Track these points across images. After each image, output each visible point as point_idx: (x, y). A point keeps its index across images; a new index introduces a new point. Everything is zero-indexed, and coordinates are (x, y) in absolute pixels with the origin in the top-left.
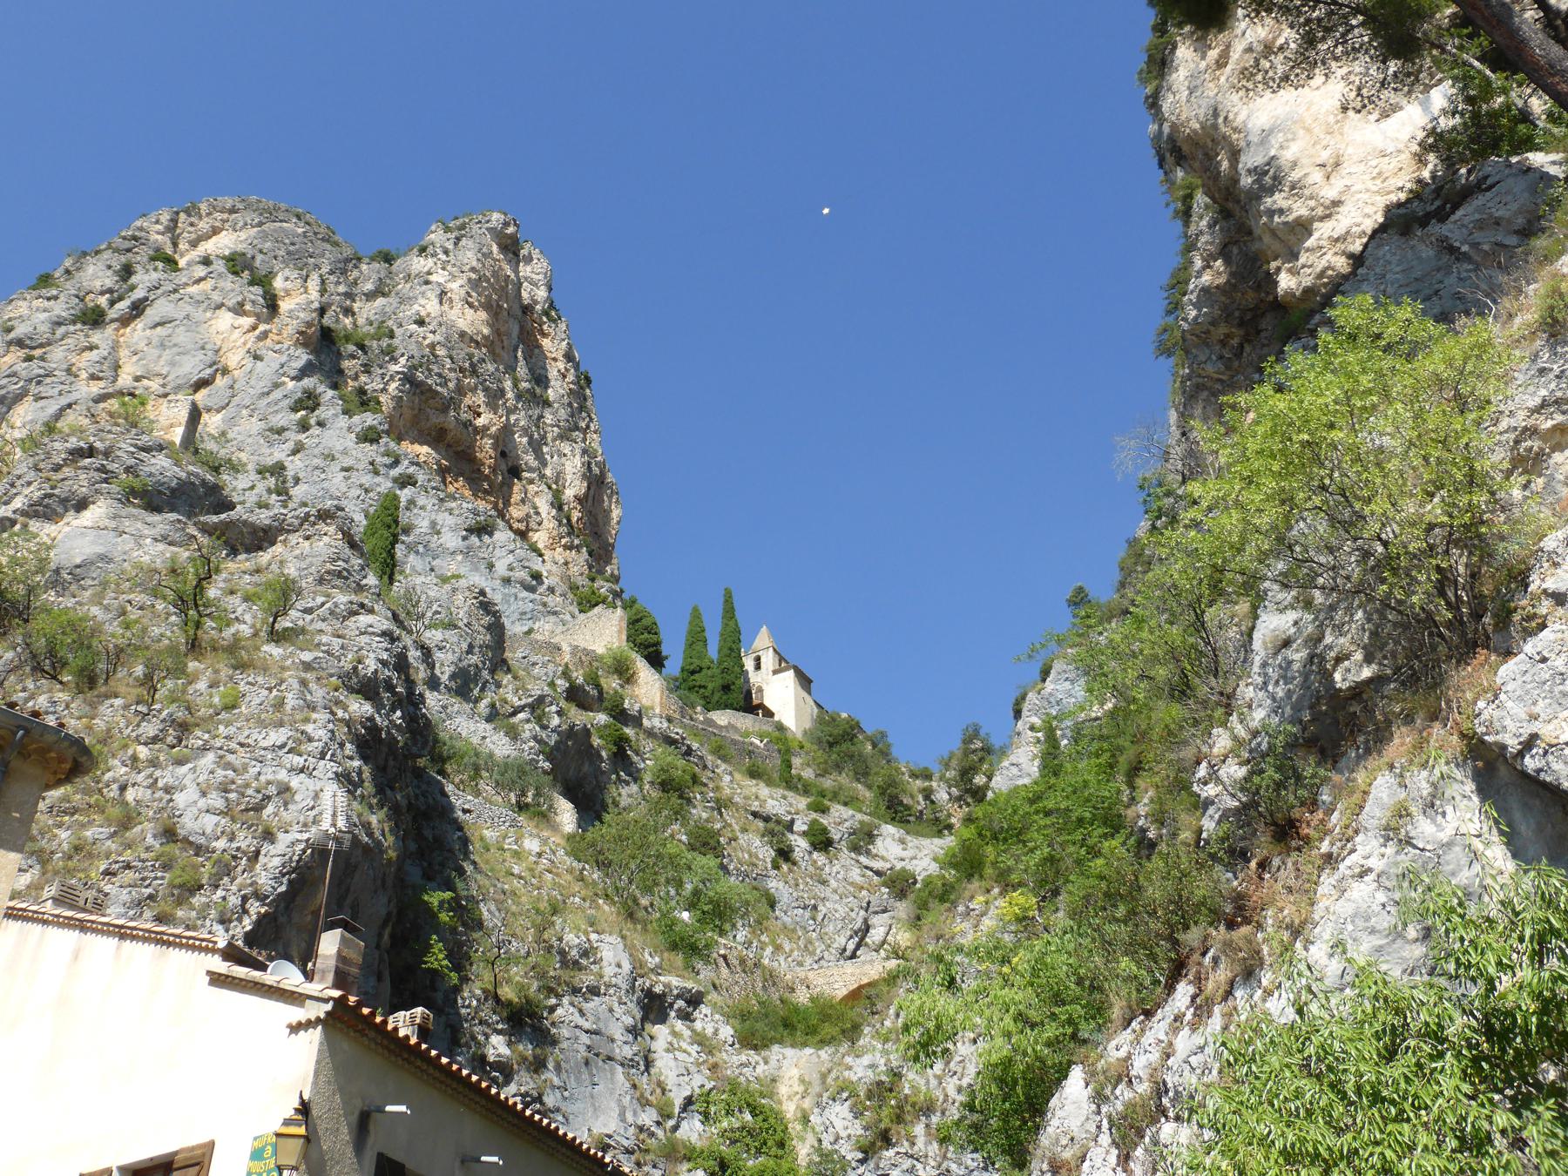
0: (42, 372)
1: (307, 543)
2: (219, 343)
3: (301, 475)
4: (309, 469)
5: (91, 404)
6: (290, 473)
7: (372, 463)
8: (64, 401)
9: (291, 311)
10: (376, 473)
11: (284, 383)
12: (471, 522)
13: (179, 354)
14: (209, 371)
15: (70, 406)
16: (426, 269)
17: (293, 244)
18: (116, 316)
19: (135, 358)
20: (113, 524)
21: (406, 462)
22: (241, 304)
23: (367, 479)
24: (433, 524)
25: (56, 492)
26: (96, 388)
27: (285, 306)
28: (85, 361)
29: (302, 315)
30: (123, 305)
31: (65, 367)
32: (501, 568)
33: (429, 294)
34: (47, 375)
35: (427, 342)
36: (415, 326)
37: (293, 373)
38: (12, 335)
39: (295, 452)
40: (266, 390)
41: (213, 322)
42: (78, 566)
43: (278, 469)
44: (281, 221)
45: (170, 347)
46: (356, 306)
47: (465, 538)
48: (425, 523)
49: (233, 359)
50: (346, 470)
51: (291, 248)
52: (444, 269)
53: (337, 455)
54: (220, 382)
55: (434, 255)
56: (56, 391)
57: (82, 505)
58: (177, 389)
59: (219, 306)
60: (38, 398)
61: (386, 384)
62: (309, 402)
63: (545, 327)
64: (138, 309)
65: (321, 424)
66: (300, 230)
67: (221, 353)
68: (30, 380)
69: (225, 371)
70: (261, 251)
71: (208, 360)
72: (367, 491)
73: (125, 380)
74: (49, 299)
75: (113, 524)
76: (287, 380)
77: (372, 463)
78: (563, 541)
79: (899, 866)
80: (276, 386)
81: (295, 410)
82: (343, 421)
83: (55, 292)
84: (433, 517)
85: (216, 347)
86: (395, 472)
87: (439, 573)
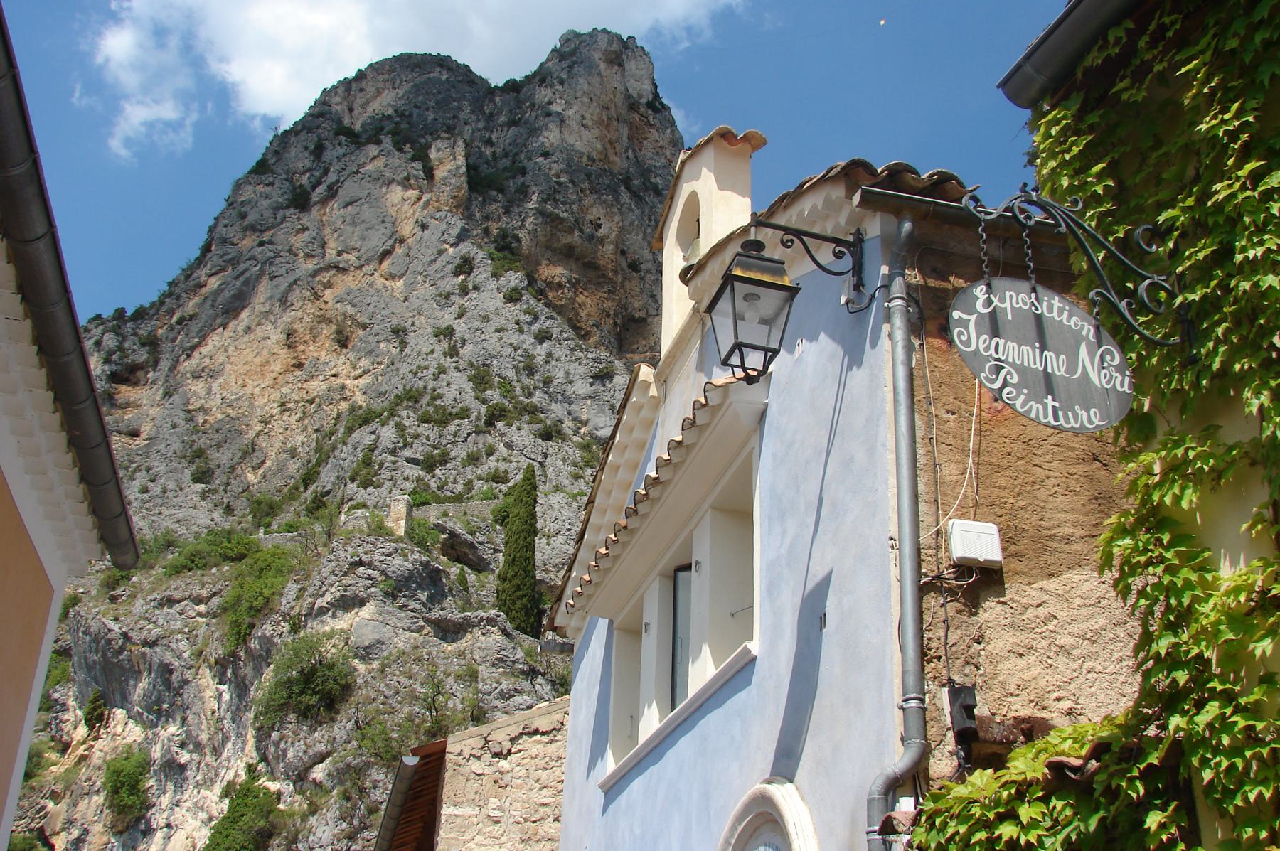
0: (271, 254)
1: (483, 638)
2: (394, 214)
3: (466, 338)
4: (472, 331)
5: (310, 279)
6: (458, 336)
7: (517, 323)
8: (291, 278)
9: (444, 179)
10: (521, 331)
11: (446, 250)
12: (596, 370)
13: (367, 229)
14: (390, 242)
15: (295, 282)
16: (547, 100)
17: (439, 92)
18: (317, 199)
19: (335, 235)
20: (380, 618)
21: (543, 318)
22: (407, 178)
23: (515, 338)
24: (567, 373)
25: (348, 593)
26: (311, 265)
27: (440, 173)
28: (299, 241)
29: (453, 181)
30: (321, 189)
31: (287, 248)
33: (550, 125)
34: (276, 257)
35: (553, 172)
36: (541, 159)
37: (452, 240)
38: (246, 222)
39: (460, 316)
40: (433, 258)
41: (388, 196)
42: (367, 647)
43: (449, 332)
44: (429, 73)
45: (360, 223)
46: (494, 137)
47: (592, 385)
48: (561, 374)
49: (407, 228)
50: (498, 331)
51: (440, 97)
52: (561, 98)
53: (491, 316)
54: (399, 251)
55: (552, 86)
56: (284, 270)
57: (362, 603)
58: (369, 261)
59: (391, 182)
60: (272, 278)
61: (523, 220)
63: (651, 119)
64: (332, 193)
65: (476, 288)
66: (444, 77)
67: (397, 223)
68: (264, 263)
69: (402, 241)
70: (416, 106)
71: (388, 232)
73: (331, 255)
74: (267, 185)
75: (380, 618)
76: (447, 246)
77: (517, 323)
80: (441, 252)
81: (456, 274)
82: (493, 284)
83: (271, 179)
84: (567, 367)
85: (393, 219)
86: (536, 327)
87: (575, 416)
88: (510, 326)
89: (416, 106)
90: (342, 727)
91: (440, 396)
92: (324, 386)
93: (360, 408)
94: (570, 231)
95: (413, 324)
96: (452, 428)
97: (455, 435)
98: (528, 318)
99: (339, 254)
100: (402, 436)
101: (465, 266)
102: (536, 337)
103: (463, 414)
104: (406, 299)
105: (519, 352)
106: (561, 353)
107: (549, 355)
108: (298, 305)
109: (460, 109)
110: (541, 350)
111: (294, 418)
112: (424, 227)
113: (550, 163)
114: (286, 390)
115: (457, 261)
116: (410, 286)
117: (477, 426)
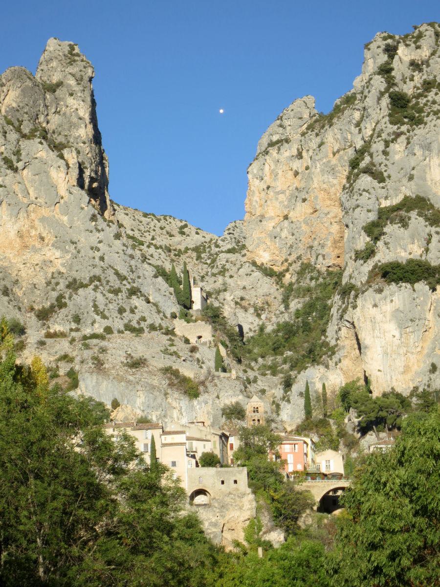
36: (82, 145)
39: (100, 242)
49: (62, 191)
53: (111, 244)
54: (62, 201)
77: (123, 251)
88: (121, 251)
92: (42, 258)
93: (63, 273)
97: (122, 299)
98: (125, 248)
99: (36, 198)
104: (71, 227)
107: (136, 266)
108: (22, 219)
109: (40, 105)
110: (133, 263)
111: (30, 272)
114: (24, 257)
115: (90, 216)
116: (71, 221)
117: (127, 296)
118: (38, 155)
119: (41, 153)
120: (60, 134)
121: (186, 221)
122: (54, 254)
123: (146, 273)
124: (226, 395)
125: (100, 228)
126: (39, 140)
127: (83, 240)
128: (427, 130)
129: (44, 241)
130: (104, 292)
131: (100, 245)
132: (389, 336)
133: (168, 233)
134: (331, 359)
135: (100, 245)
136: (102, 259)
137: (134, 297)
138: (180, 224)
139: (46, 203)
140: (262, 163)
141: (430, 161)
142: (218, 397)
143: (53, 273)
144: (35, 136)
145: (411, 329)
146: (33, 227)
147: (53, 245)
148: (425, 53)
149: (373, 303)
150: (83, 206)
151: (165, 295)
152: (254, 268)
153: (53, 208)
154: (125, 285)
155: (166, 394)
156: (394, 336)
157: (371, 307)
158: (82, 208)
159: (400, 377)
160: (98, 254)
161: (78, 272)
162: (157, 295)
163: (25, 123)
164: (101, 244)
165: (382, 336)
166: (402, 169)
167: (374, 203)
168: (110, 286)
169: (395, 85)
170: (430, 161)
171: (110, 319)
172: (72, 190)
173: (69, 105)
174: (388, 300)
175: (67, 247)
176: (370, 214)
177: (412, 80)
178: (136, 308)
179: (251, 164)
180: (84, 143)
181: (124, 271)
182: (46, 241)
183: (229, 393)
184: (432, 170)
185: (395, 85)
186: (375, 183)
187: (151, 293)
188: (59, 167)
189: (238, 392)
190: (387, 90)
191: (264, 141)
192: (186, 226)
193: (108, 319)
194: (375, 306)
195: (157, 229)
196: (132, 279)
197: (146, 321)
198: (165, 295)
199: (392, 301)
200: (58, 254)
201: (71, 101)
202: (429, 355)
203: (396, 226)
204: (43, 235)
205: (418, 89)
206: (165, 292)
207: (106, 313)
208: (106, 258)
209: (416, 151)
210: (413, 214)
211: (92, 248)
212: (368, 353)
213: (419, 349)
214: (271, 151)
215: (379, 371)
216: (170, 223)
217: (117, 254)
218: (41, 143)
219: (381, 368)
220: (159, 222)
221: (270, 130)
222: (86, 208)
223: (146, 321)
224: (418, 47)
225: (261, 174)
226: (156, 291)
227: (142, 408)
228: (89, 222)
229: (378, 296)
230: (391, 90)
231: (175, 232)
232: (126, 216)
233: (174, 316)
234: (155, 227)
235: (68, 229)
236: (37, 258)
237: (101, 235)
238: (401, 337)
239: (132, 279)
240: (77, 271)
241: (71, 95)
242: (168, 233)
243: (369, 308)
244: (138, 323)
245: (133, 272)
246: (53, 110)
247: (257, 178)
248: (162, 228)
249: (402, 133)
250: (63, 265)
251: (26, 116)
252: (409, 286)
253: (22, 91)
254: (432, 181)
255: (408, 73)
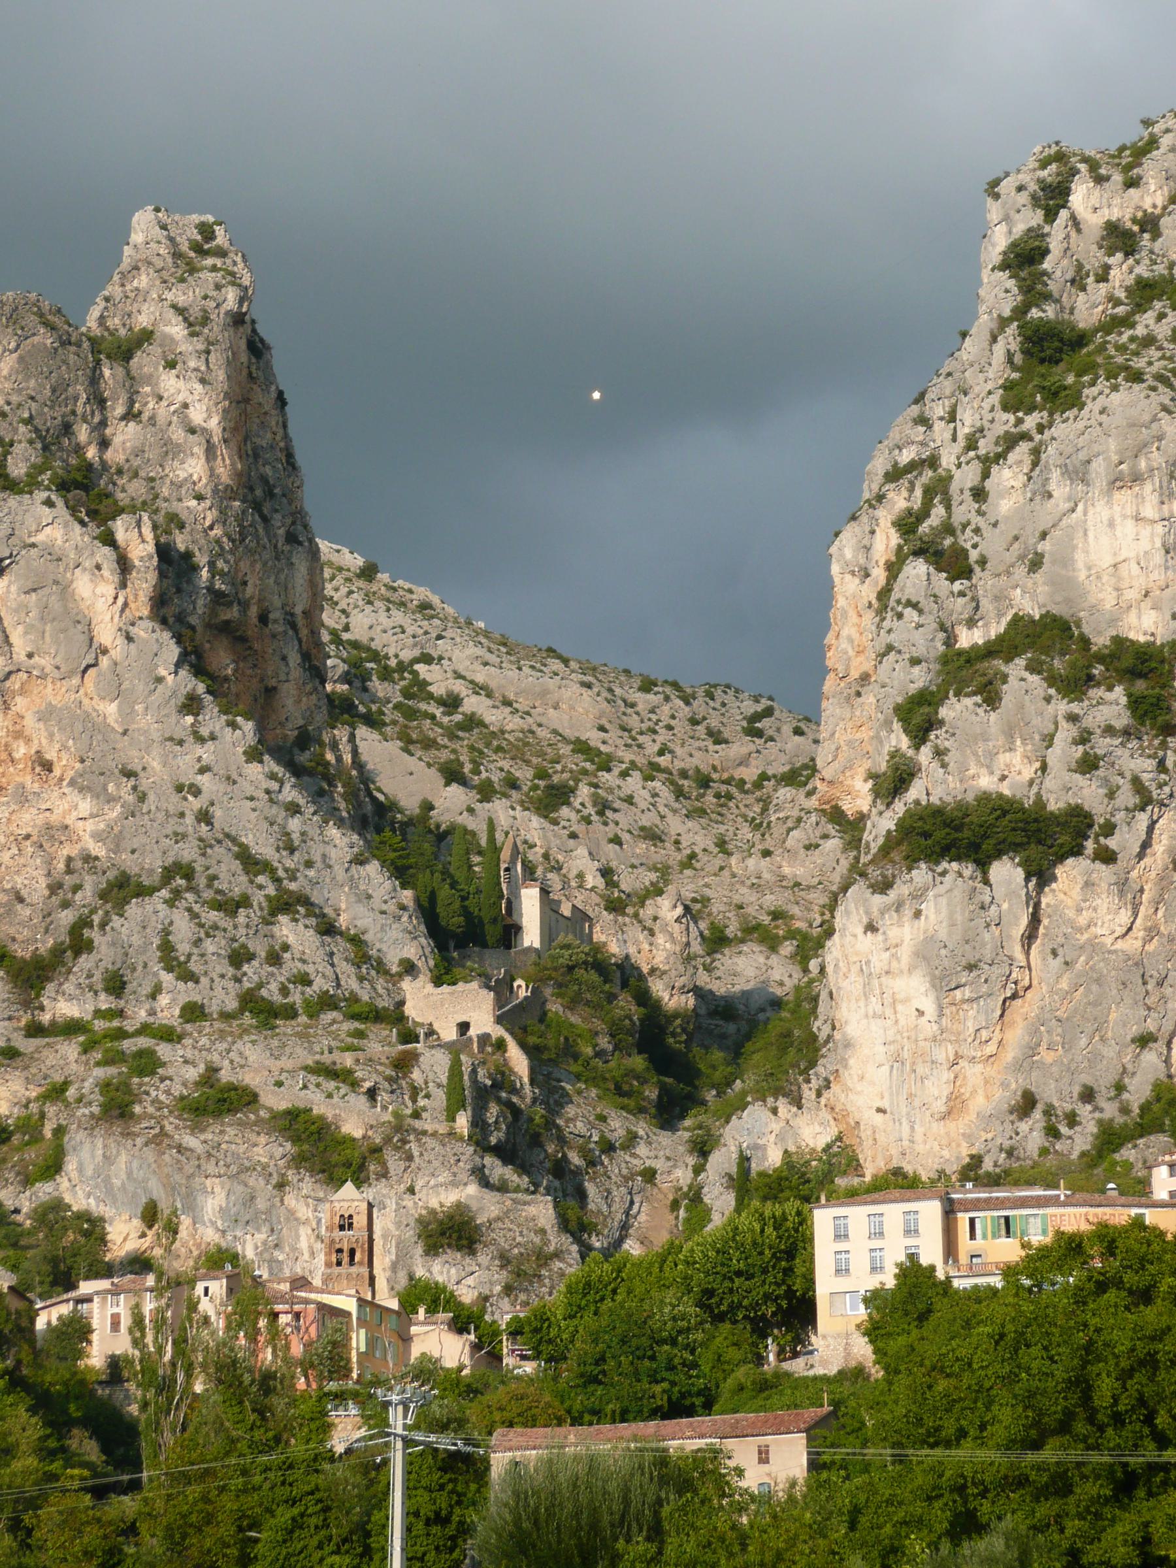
19: (20, 628)
24: (324, 856)
32: (376, 903)
36: (194, 503)
39: (203, 770)
49: (106, 634)
50: (252, 799)
53: (235, 776)
54: (104, 662)
61: (194, 603)
62: (191, 705)
65: (213, 737)
69: (105, 651)
72: (272, 824)
77: (268, 792)
78: (309, 687)
79: (648, 1163)
89: (32, 398)
90: (483, 1258)
91: (214, 878)
92: (40, 820)
93: (97, 858)
94: (229, 605)
95: (144, 769)
96: (242, 916)
97: (247, 926)
98: (274, 786)
99: (30, 656)
100: (202, 926)
101: (191, 705)
102: (287, 810)
103: (244, 902)
104: (125, 733)
105: (276, 828)
106: (313, 832)
107: (303, 834)
109: (76, 399)
110: (294, 824)
112: (129, 639)
113: (204, 510)
115: (181, 699)
116: (127, 714)
117: (263, 918)
118: (40, 538)
119: (48, 530)
120: (136, 475)
121: (771, 699)
122: (76, 807)
123: (333, 854)
124: (432, 1183)
125: (205, 732)
126: (45, 494)
127: (156, 765)
128: (1080, 425)
129: (50, 771)
130: (197, 908)
131: (204, 781)
132: (906, 1013)
133: (710, 733)
134: (808, 1081)
135: (204, 781)
136: (204, 817)
137: (283, 919)
138: (750, 707)
139: (58, 668)
140: (867, 529)
141: (1085, 513)
142: (411, 1190)
143: (69, 859)
144: (39, 485)
145: (967, 992)
146: (18, 735)
147: (72, 783)
148: (1152, 196)
149: (865, 920)
150: (162, 672)
151: (383, 912)
152: (830, 829)
153: (76, 681)
154: (260, 887)
155: (281, 1186)
156: (921, 1013)
157: (860, 930)
158: (160, 680)
159: (938, 1128)
160: (195, 803)
161: (136, 855)
162: (361, 909)
163: (18, 449)
164: (207, 776)
165: (889, 1012)
166: (1016, 538)
167: (932, 640)
168: (218, 892)
169: (1047, 297)
170: (1085, 513)
171: (204, 981)
172: (134, 631)
173: (165, 395)
174: (908, 912)
175: (111, 788)
176: (916, 670)
177: (1103, 278)
178: (286, 947)
179: (837, 535)
180: (200, 498)
181: (263, 847)
182: (57, 772)
183: (441, 1179)
184: (1091, 534)
185: (1047, 297)
186: (941, 581)
187: (343, 906)
188: (98, 567)
189: (464, 1176)
190: (1020, 312)
191: (879, 465)
192: (768, 712)
193: (197, 982)
194: (871, 928)
195: (681, 726)
196: (286, 870)
197: (309, 983)
198: (383, 912)
199: (918, 914)
200: (85, 806)
201: (169, 383)
202: (1018, 1066)
203: (968, 702)
204: (48, 757)
205: (1117, 303)
206: (386, 902)
207: (195, 966)
208: (218, 813)
209: (1052, 486)
210: (1016, 668)
211: (179, 789)
212: (851, 1062)
213: (991, 1049)
214: (890, 495)
215: (880, 1110)
216: (724, 705)
217: (249, 804)
218: (49, 503)
219: (885, 1104)
220: (688, 703)
221: (895, 435)
222: (170, 679)
223: (309, 983)
224: (1132, 183)
225: (862, 561)
226: (359, 901)
227: (219, 1223)
228: (174, 717)
229: (878, 900)
230: (1034, 313)
231: (733, 728)
232: (584, 690)
233: (409, 968)
234: (673, 717)
235: (118, 737)
236: (29, 820)
237: (206, 753)
238: (941, 1015)
239: (286, 870)
240: (133, 852)
241: (171, 365)
242: (710, 733)
243: (855, 936)
244: (284, 991)
245: (292, 850)
246: (120, 410)
247: (853, 573)
248: (694, 722)
249: (1025, 436)
250: (97, 836)
251: (22, 429)
252: (969, 869)
253: (21, 359)
254: (1089, 569)
255: (1094, 258)
